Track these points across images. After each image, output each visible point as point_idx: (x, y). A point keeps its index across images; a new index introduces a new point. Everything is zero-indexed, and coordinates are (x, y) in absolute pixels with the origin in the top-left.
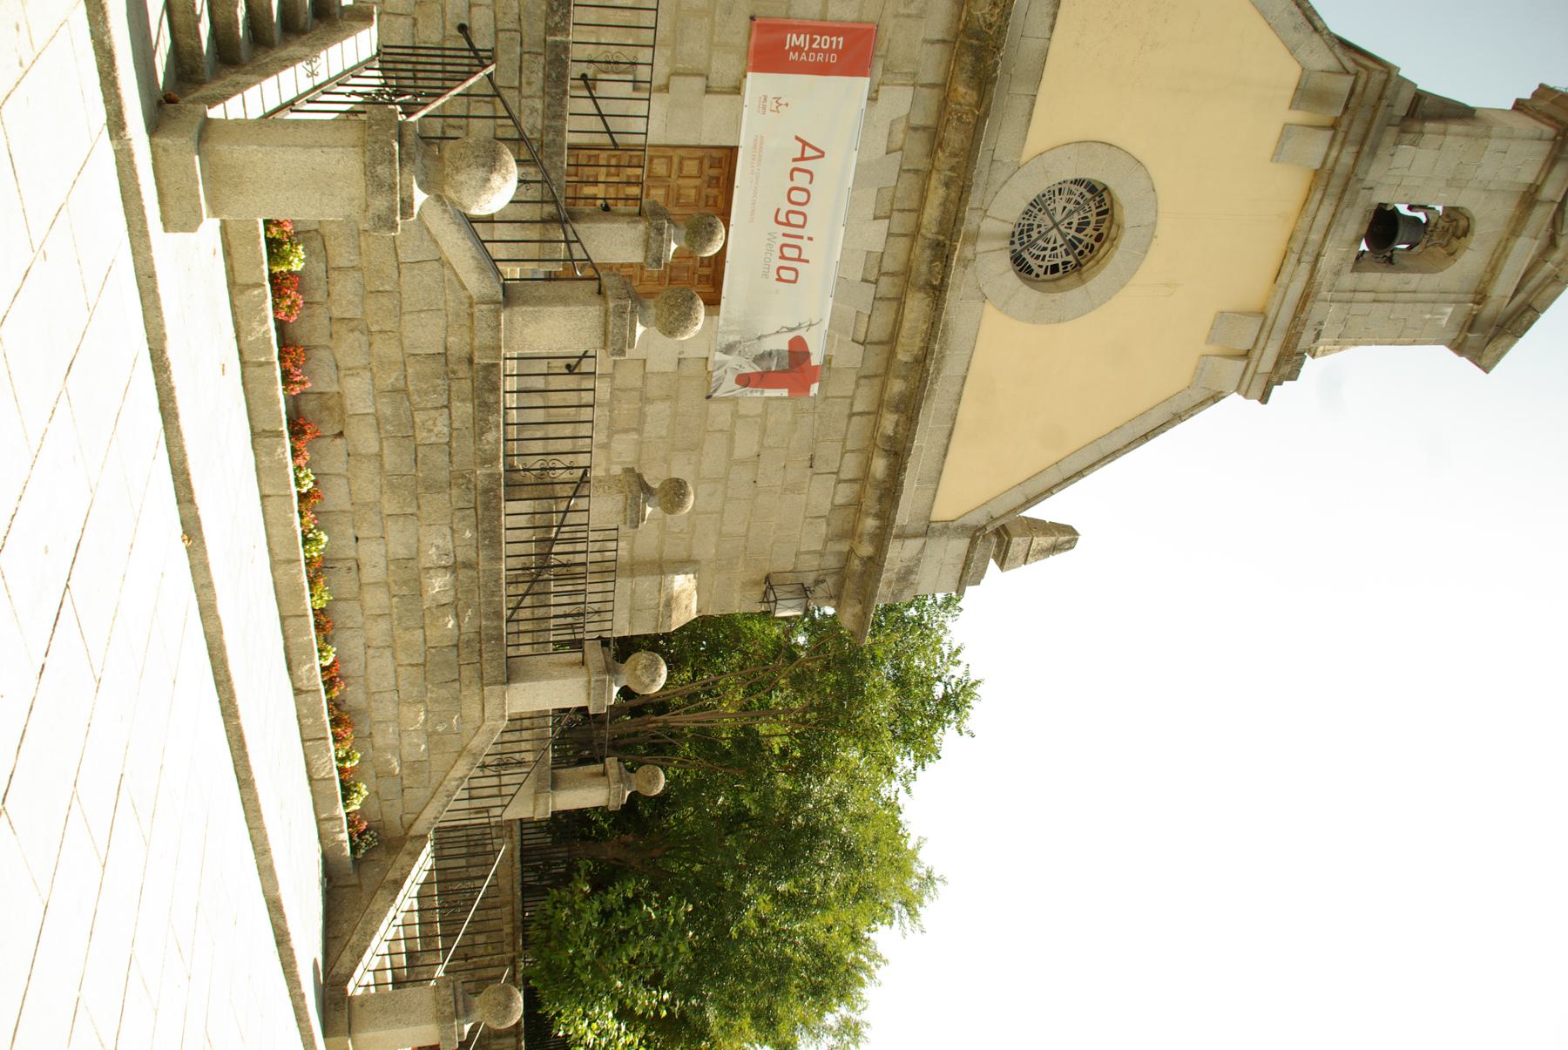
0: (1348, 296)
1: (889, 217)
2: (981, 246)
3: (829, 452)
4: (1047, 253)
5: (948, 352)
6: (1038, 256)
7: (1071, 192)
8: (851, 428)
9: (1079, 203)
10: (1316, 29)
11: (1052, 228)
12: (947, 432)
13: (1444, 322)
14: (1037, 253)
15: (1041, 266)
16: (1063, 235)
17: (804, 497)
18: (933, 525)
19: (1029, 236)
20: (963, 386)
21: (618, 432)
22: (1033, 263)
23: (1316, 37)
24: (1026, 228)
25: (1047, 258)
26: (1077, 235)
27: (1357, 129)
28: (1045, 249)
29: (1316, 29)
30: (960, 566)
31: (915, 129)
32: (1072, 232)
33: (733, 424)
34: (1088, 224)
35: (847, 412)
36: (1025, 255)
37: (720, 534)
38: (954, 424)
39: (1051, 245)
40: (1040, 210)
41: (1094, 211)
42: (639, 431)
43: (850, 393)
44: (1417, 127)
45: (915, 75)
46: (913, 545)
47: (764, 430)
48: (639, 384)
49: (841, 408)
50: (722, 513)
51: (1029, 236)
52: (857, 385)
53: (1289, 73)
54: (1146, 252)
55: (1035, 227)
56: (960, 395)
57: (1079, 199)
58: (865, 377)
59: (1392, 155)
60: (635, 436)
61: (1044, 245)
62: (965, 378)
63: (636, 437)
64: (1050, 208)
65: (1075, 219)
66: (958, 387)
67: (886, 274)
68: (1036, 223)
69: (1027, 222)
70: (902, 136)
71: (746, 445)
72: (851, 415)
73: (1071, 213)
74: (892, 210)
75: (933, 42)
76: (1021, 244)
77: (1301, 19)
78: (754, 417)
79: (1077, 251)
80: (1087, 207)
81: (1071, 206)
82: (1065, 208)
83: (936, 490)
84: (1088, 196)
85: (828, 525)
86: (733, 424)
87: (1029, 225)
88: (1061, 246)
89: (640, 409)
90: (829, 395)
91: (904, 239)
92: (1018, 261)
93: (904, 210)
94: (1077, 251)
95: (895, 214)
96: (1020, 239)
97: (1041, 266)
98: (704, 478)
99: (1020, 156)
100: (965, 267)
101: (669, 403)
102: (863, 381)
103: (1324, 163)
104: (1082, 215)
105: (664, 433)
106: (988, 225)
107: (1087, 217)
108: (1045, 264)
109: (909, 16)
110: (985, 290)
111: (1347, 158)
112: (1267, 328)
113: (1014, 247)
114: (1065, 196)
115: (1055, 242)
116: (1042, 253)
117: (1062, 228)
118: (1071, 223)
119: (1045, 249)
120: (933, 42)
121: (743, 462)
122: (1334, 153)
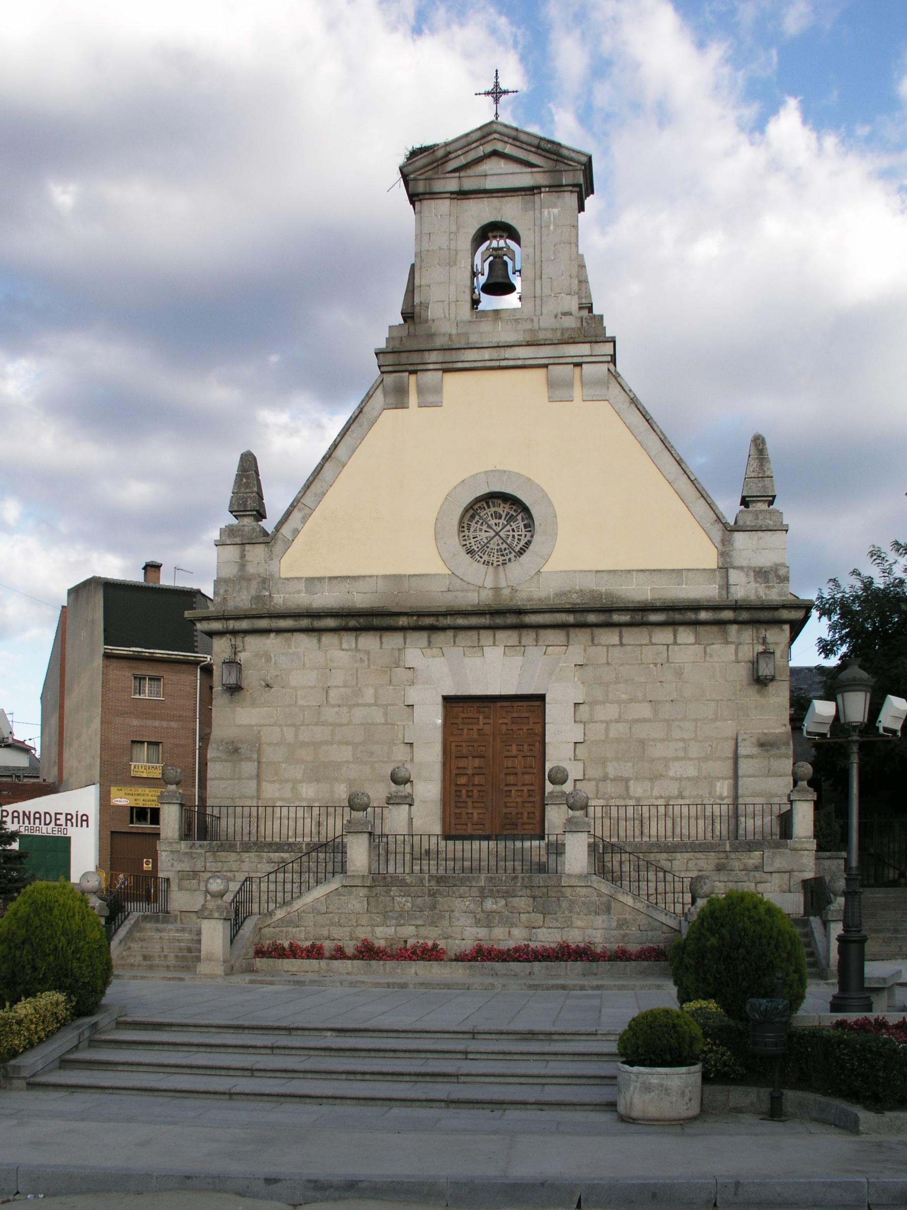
0: (538, 301)
1: (482, 646)
2: (503, 584)
3: (649, 653)
4: (516, 534)
5: (577, 588)
6: (519, 540)
7: (475, 531)
8: (632, 643)
9: (482, 523)
10: (361, 412)
11: (500, 536)
12: (640, 573)
13: (556, 211)
14: (516, 540)
15: (526, 536)
16: (505, 526)
17: (686, 665)
18: (720, 565)
19: (505, 549)
20: (603, 571)
21: (628, 793)
22: (522, 543)
23: (364, 410)
24: (499, 553)
25: (520, 533)
26: (503, 517)
27: (415, 358)
28: (513, 536)
29: (361, 412)
30: (760, 533)
31: (429, 642)
32: (501, 521)
33: (626, 721)
34: (495, 512)
35: (619, 648)
36: (517, 549)
37: (715, 719)
38: (633, 570)
39: (511, 533)
40: (488, 547)
41: (487, 510)
42: (627, 780)
43: (605, 648)
44: (417, 309)
45: (399, 650)
46: (735, 577)
47: (631, 700)
48: (593, 783)
49: (617, 653)
50: (695, 720)
51: (505, 549)
52: (599, 645)
53: (389, 416)
54: (505, 471)
55: (499, 547)
56: (610, 572)
57: (479, 523)
58: (593, 640)
59: (434, 320)
60: (631, 783)
61: (511, 537)
62: (597, 572)
63: (632, 782)
64: (486, 541)
65: (492, 522)
66: (604, 574)
67: (520, 643)
68: (497, 547)
69: (496, 553)
70: (434, 649)
71: (645, 711)
72: (622, 644)
73: (489, 526)
74: (478, 646)
75: (381, 643)
76: (510, 553)
77: (355, 424)
78: (620, 708)
79: (515, 514)
80: (485, 517)
81: (485, 527)
82: (486, 531)
83: (689, 570)
84: (477, 518)
85: (713, 644)
86: (626, 721)
87: (497, 552)
88: (511, 526)
89: (612, 780)
90: (605, 662)
91: (496, 635)
92: (521, 552)
93: (479, 639)
94: (515, 514)
95: (480, 644)
96: (507, 555)
97: (526, 536)
98: (667, 735)
99: (445, 575)
100: (516, 591)
101: (609, 763)
102: (596, 642)
103: (439, 370)
104: (490, 518)
105: (630, 764)
106: (489, 583)
107: (492, 515)
108: (523, 533)
109: (369, 659)
110: (533, 573)
111: (433, 357)
112: (557, 361)
113: (513, 559)
114: (478, 533)
115: (509, 531)
116: (516, 537)
117: (499, 529)
118: (496, 524)
119: (513, 536)
120: (381, 643)
121: (656, 712)
122: (431, 367)
